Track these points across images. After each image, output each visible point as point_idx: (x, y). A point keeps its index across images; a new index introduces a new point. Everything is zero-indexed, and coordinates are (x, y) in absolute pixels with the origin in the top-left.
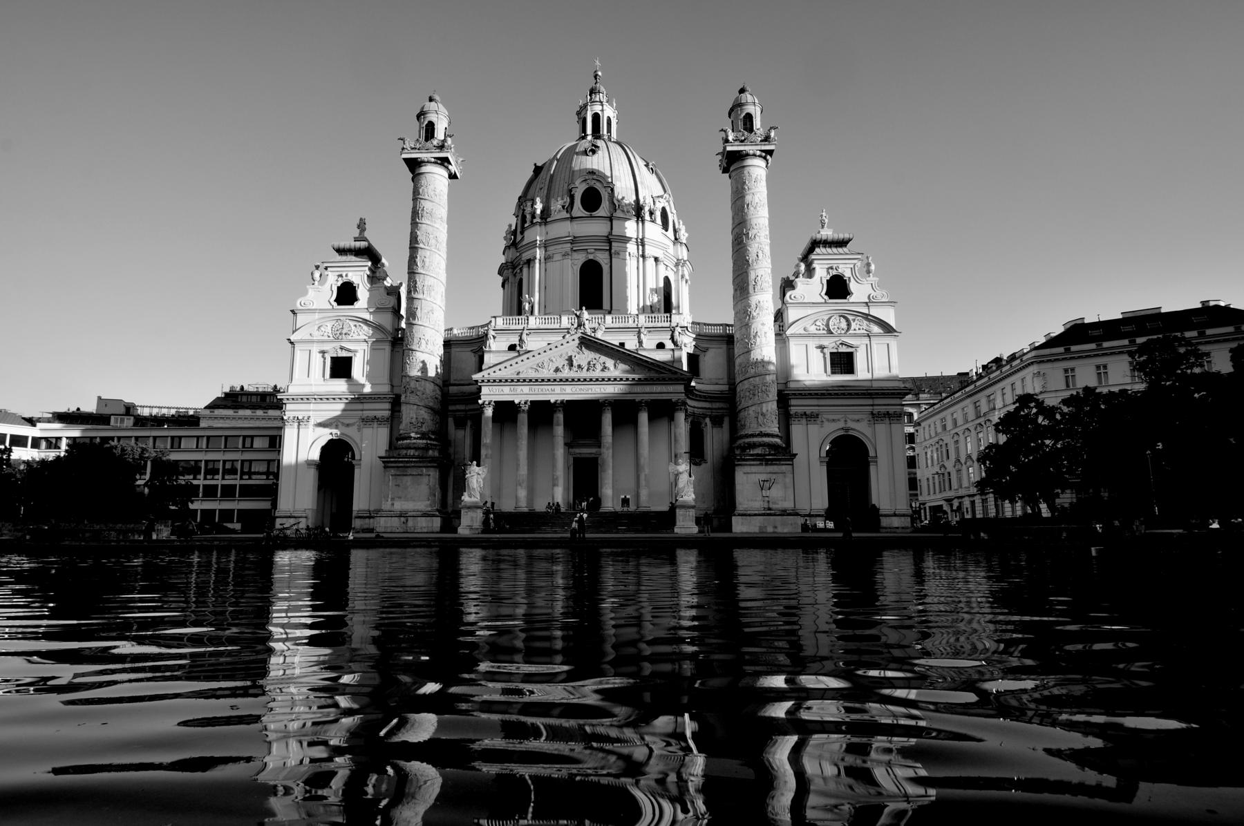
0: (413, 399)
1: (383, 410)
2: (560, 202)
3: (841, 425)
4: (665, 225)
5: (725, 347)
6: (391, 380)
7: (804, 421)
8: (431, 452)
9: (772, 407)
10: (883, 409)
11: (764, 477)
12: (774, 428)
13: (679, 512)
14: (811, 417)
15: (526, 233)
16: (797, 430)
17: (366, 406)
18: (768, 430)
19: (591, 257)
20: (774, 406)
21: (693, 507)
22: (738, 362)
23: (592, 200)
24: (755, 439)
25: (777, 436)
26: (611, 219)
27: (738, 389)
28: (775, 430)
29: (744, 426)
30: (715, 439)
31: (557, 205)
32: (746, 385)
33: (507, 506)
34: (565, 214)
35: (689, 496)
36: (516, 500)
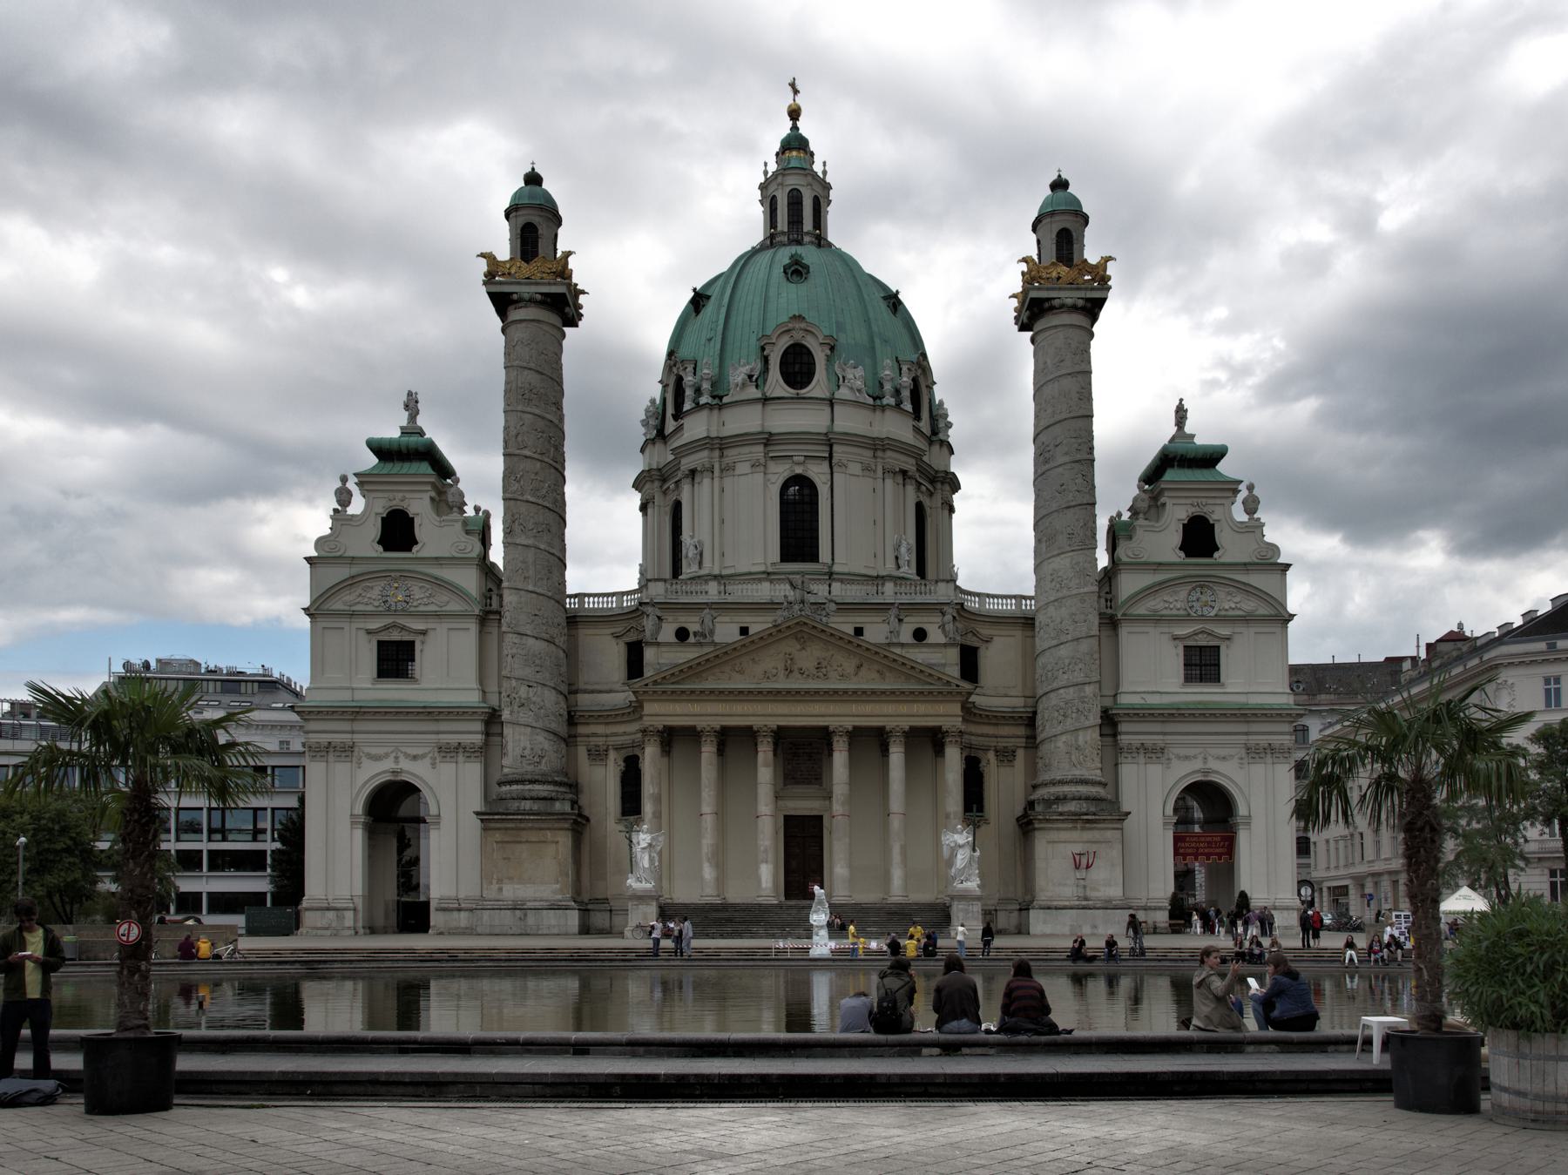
0: (525, 716)
1: (473, 734)
2: (745, 370)
3: (1198, 765)
4: (917, 415)
5: (1018, 633)
6: (482, 679)
7: (1141, 759)
8: (558, 806)
9: (1090, 738)
10: (1263, 740)
11: (1078, 848)
12: (1092, 770)
13: (957, 910)
14: (1154, 753)
15: (687, 422)
16: (1130, 772)
17: (443, 726)
18: (1087, 775)
19: (799, 470)
20: (1096, 734)
21: (978, 898)
22: (1041, 661)
23: (798, 367)
24: (1066, 789)
25: (1100, 783)
26: (831, 402)
27: (1040, 707)
28: (1096, 775)
29: (1048, 766)
30: (1005, 787)
31: (737, 375)
32: (1053, 700)
33: (684, 893)
34: (753, 392)
35: (973, 885)
36: (699, 885)
